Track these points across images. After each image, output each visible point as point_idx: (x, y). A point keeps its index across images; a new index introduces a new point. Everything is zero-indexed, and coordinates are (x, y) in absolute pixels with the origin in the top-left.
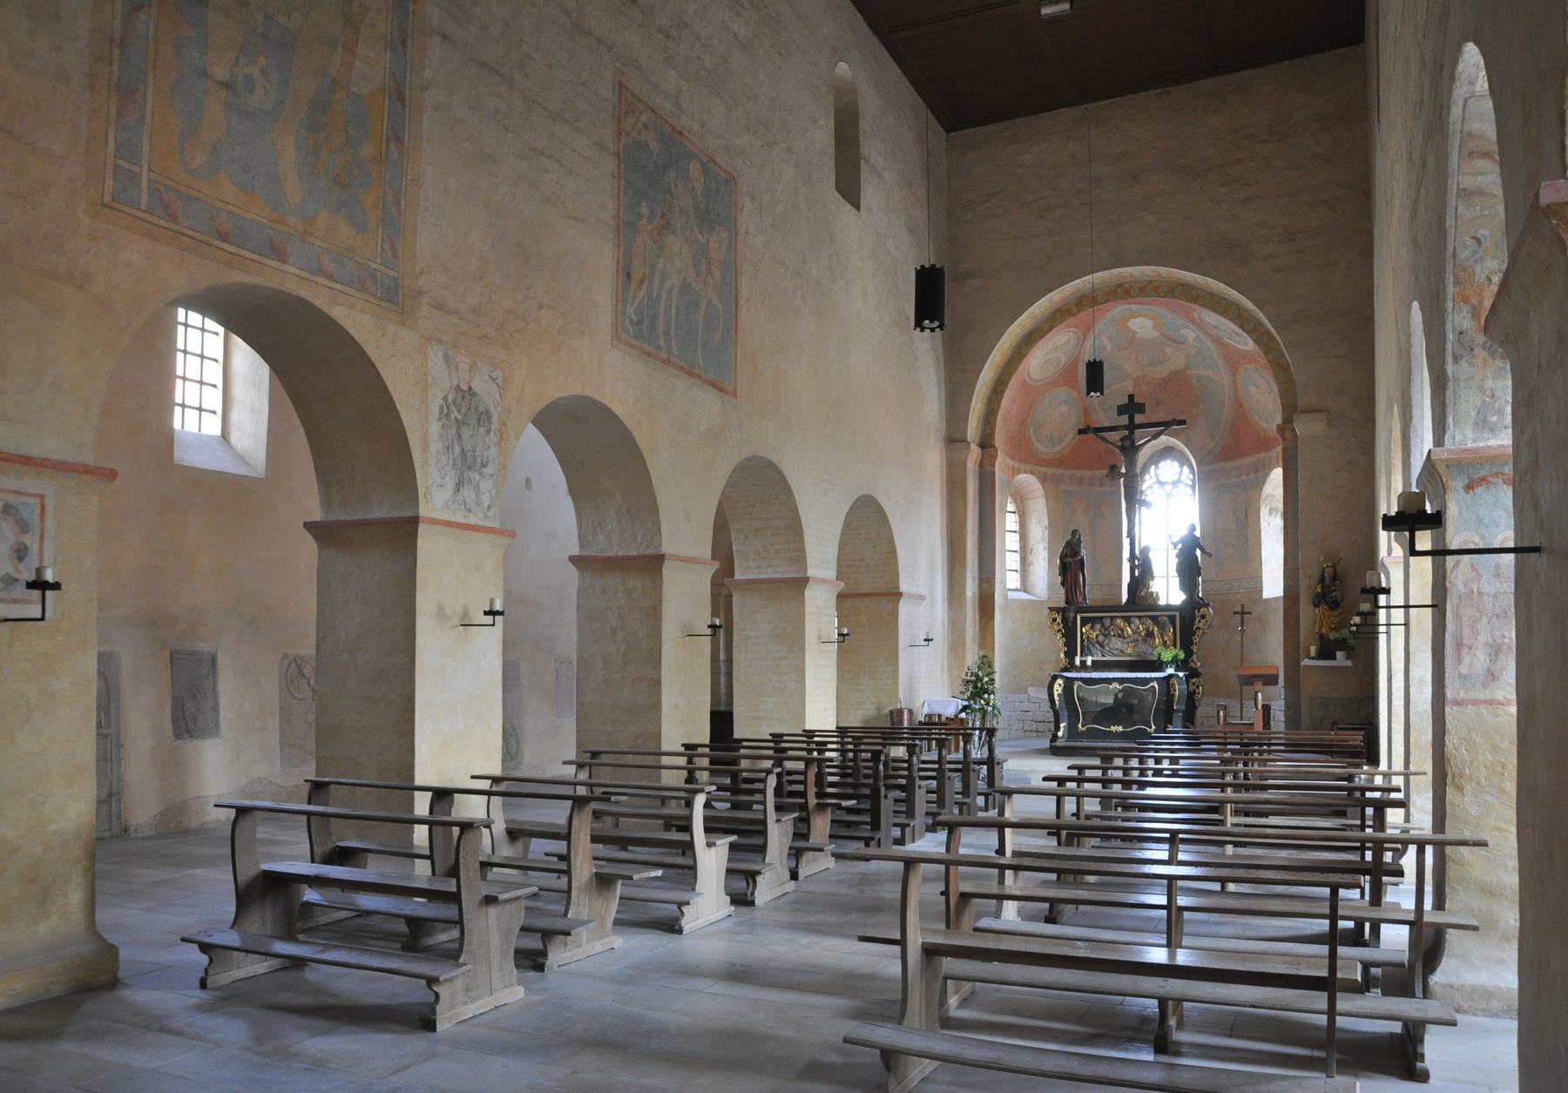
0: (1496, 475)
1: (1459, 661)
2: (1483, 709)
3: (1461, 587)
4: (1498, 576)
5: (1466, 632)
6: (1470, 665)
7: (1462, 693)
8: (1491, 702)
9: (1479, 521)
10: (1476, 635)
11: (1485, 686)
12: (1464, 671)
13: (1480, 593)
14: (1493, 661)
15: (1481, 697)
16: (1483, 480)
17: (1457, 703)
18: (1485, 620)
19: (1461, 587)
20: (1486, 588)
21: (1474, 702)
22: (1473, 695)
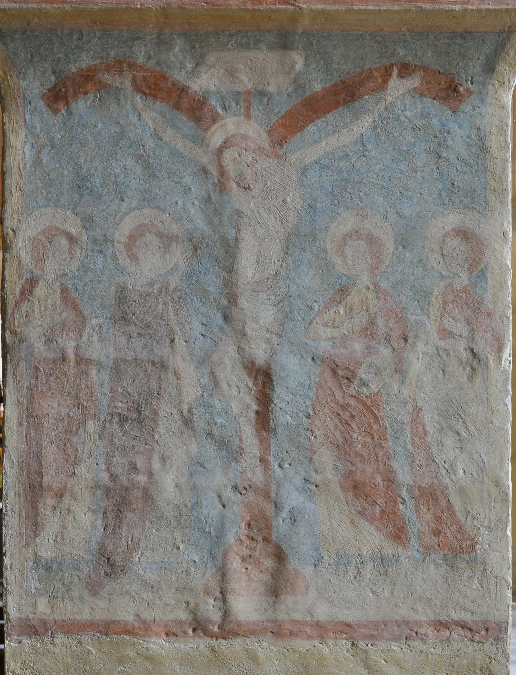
0: (118, 66)
1: (34, 524)
2: (89, 642)
3: (39, 345)
4: (122, 319)
5: (51, 454)
6: (61, 538)
7: (42, 607)
8: (108, 628)
9: (81, 183)
10: (71, 462)
11: (94, 588)
12: (46, 552)
13: (80, 360)
14: (112, 529)
15: (85, 614)
16: (88, 78)
17: (33, 629)
18: (92, 427)
19: (39, 345)
20: (96, 349)
21: (71, 628)
22: (67, 611)
